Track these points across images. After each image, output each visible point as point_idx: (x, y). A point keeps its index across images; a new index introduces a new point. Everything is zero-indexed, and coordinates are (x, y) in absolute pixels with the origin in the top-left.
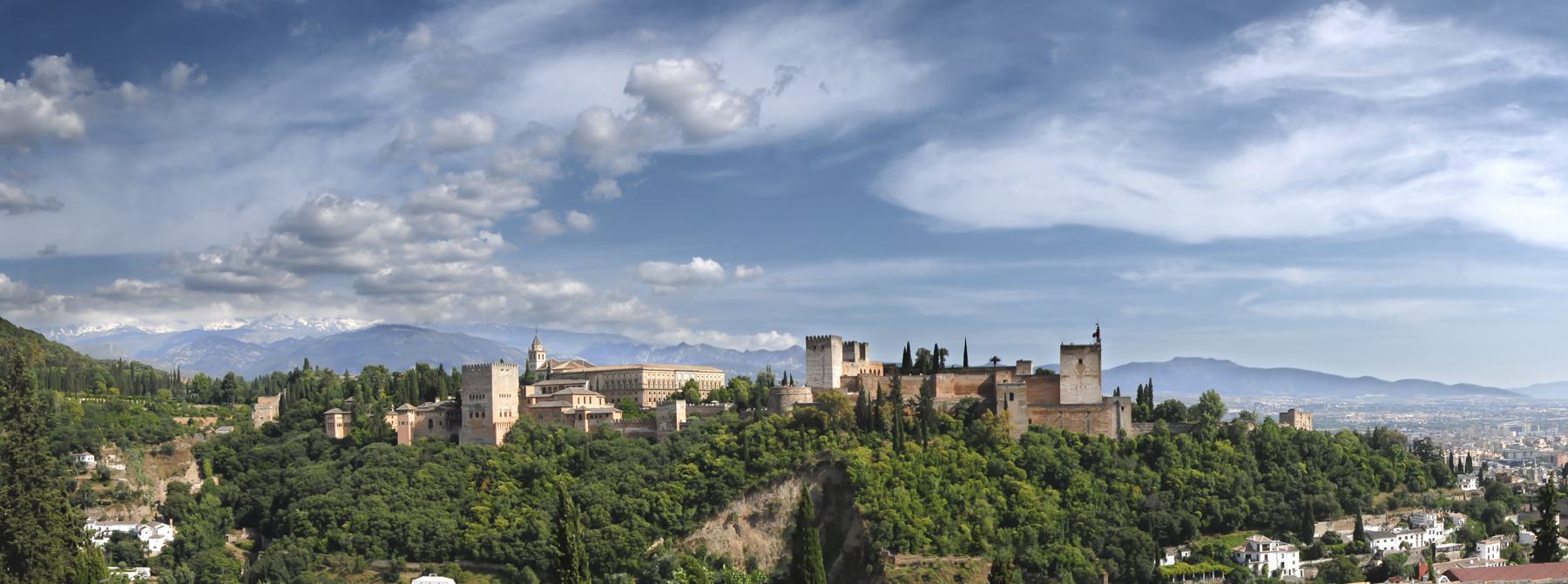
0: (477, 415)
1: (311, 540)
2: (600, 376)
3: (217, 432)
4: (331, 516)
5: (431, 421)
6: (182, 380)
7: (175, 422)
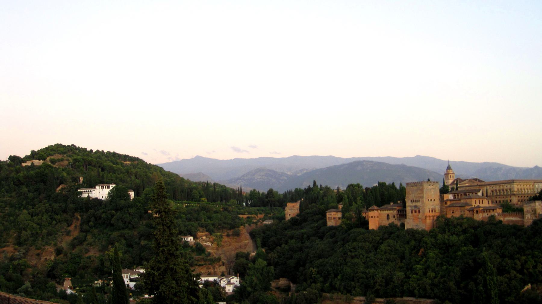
0: (415, 212)
1: (319, 285)
2: (488, 187)
3: (264, 223)
4: (331, 271)
5: (388, 215)
6: (243, 194)
7: (239, 218)
